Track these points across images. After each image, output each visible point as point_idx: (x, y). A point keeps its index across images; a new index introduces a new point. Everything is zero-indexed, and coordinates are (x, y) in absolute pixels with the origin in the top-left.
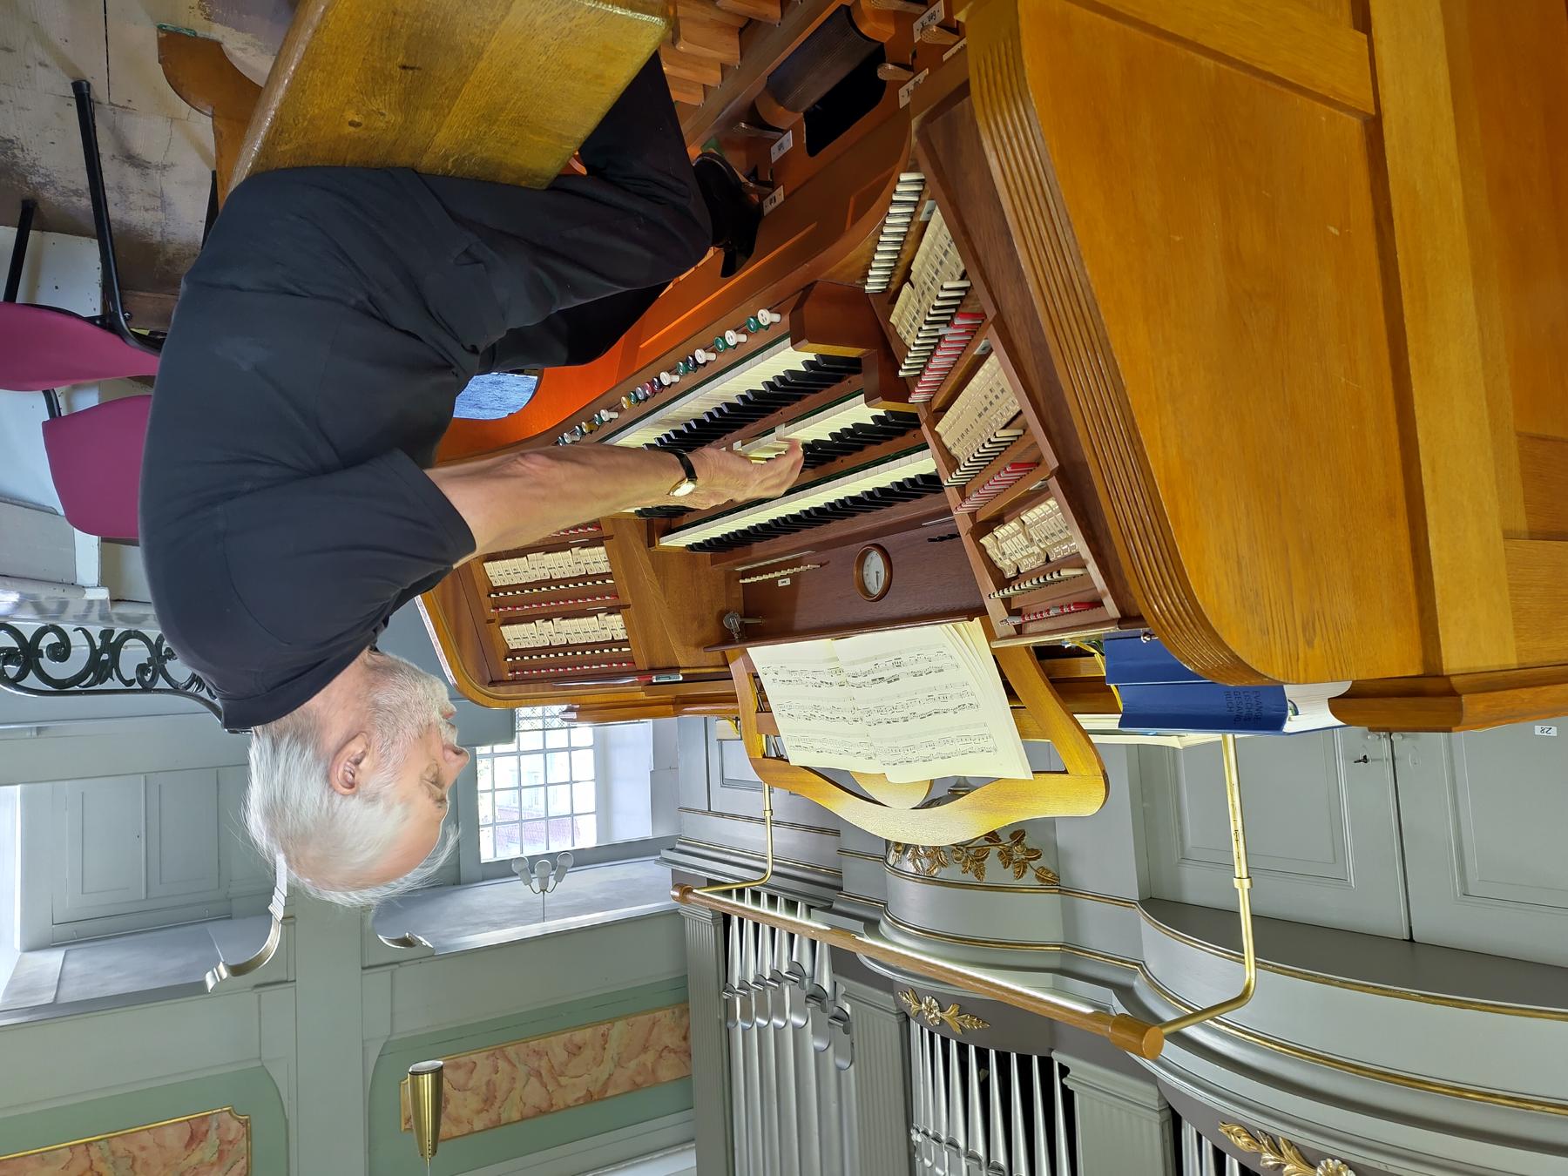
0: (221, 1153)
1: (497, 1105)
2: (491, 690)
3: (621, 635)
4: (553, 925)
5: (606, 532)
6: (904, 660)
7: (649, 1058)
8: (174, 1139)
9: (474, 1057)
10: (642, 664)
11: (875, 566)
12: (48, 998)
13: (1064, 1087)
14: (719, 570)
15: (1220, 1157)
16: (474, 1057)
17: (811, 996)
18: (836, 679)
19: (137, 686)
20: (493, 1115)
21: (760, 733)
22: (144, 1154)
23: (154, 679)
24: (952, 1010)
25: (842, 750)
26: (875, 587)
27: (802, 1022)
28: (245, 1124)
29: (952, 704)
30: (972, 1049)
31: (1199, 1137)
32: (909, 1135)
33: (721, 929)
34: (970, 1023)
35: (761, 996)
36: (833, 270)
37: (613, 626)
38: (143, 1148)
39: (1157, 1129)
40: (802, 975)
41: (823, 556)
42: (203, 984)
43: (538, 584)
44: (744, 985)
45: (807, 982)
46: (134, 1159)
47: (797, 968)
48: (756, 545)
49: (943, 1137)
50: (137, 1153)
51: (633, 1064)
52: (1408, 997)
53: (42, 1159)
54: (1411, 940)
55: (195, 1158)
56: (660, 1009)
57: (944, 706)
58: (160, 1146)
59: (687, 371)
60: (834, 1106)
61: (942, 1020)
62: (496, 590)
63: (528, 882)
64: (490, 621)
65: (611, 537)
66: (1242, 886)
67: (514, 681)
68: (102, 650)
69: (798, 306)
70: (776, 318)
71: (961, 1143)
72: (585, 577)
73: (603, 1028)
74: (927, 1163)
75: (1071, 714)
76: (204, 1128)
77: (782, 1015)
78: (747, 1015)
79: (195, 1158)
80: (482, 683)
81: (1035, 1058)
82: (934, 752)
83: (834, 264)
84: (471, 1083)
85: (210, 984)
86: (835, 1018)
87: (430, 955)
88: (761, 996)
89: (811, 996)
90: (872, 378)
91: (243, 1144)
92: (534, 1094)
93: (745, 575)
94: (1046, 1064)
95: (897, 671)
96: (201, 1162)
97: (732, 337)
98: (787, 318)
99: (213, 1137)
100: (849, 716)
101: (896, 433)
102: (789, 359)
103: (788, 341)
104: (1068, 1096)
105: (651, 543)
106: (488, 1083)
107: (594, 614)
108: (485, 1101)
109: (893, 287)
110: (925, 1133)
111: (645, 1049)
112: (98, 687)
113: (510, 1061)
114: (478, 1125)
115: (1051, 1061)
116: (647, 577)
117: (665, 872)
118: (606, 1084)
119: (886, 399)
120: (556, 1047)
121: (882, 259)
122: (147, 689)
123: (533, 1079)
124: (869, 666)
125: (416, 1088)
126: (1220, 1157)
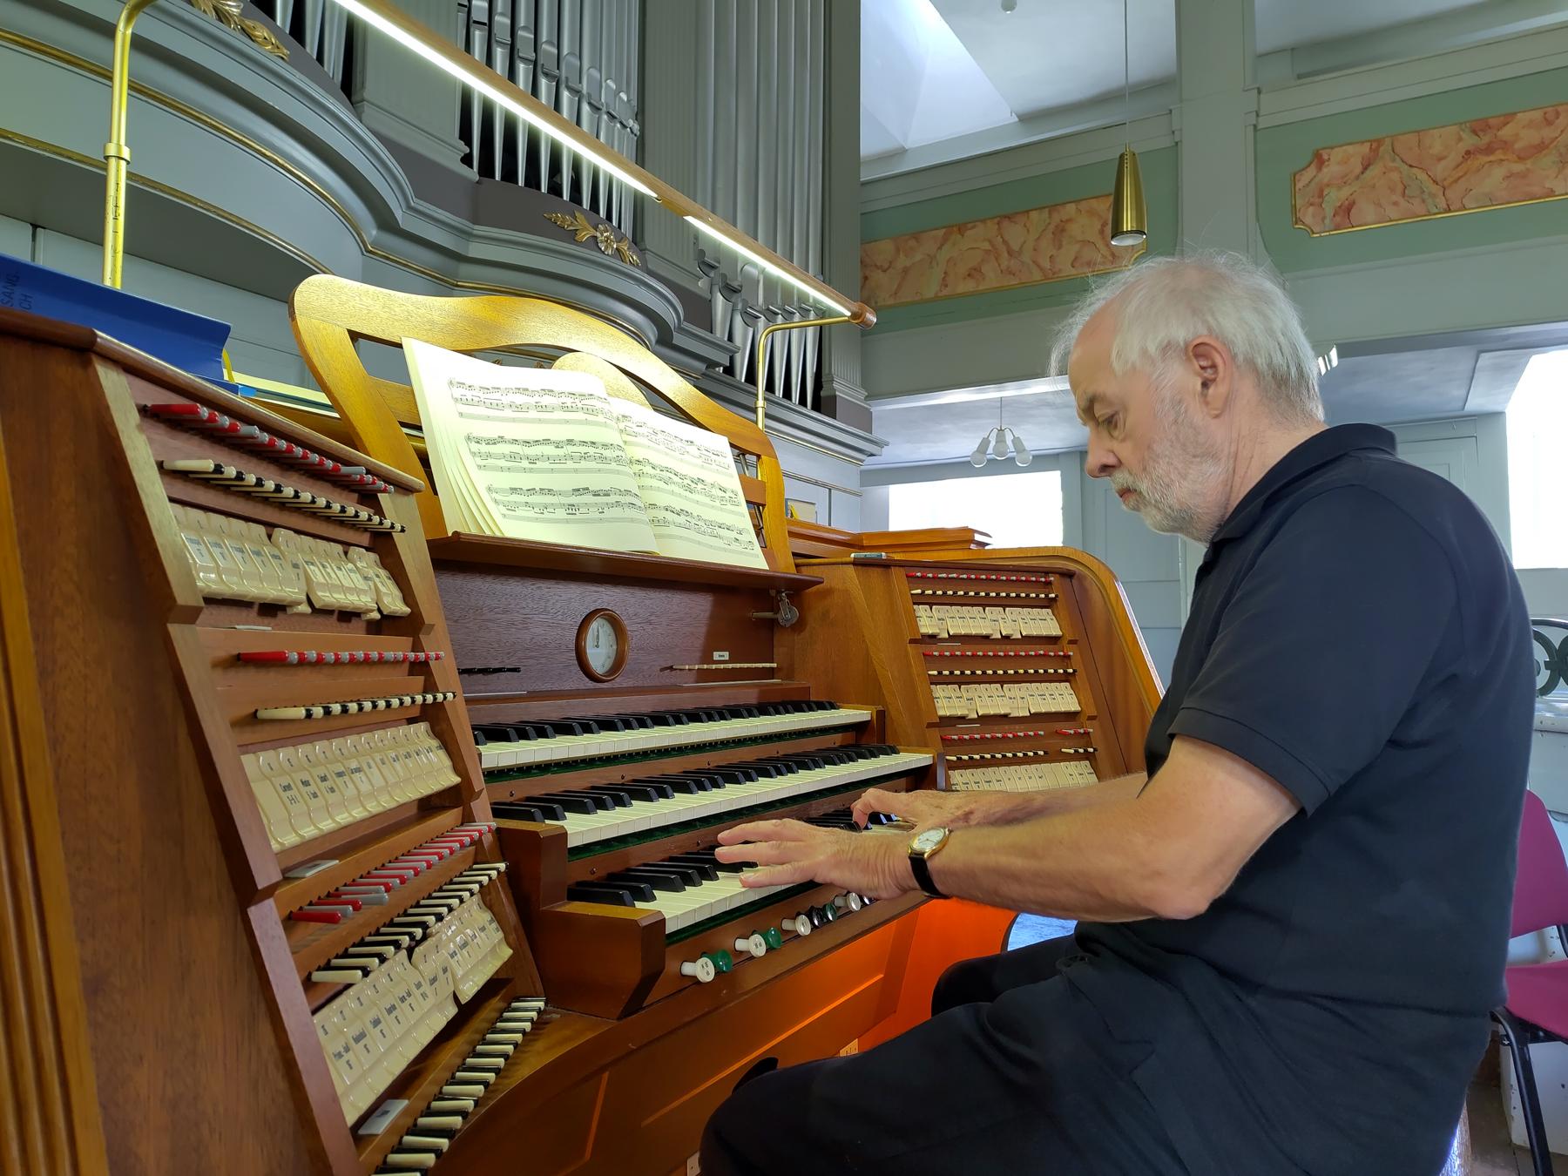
0: (1321, 195)
1: (1052, 227)
2: (1072, 567)
3: (922, 611)
4: (991, 393)
5: (935, 734)
6: (561, 513)
7: (902, 261)
8: (1366, 211)
9: (1073, 271)
10: (898, 575)
11: (600, 654)
12: (1485, 358)
13: (469, 143)
14: (794, 684)
15: (297, 29)
16: (1073, 271)
17: (736, 291)
18: (661, 514)
20: (1056, 218)
21: (762, 484)
22: (1394, 198)
24: (584, 236)
25: (660, 436)
26: (599, 628)
30: (566, 196)
31: (320, 58)
32: (642, 130)
33: (825, 371)
34: (567, 221)
36: (590, 1035)
37: (929, 621)
38: (1395, 204)
39: (368, 84)
40: (745, 313)
41: (668, 679)
42: (1340, 356)
43: (1017, 679)
46: (1404, 194)
48: (753, 701)
49: (605, 117)
50: (1401, 200)
51: (918, 257)
52: (28, 140)
53: (1492, 200)
54: (35, 226)
55: (1345, 192)
56: (891, 306)
58: (1380, 205)
59: (824, 909)
60: (720, 185)
61: (596, 228)
62: (1066, 678)
63: (1016, 441)
64: (1072, 642)
65: (930, 725)
66: (119, 145)
67: (1047, 573)
69: (649, 980)
70: (688, 968)
71: (586, 108)
72: (961, 681)
73: (945, 292)
74: (624, 96)
75: (344, 417)
76: (1338, 219)
80: (1082, 578)
81: (498, 176)
82: (537, 398)
83: (575, 1033)
84: (1077, 247)
85: (1334, 353)
86: (713, 267)
89: (736, 291)
90: (551, 872)
92: (1015, 234)
93: (770, 673)
94: (486, 169)
96: (1340, 188)
97: (755, 945)
98: (670, 966)
99: (1329, 212)
100: (648, 469)
101: (536, 798)
102: (677, 907)
103: (670, 928)
104: (465, 135)
105: (881, 715)
106: (1060, 247)
107: (952, 638)
108: (1063, 230)
109: (496, 1003)
110: (624, 126)
111: (906, 271)
114: (1071, 208)
115: (481, 173)
116: (888, 673)
117: (877, 434)
118: (945, 240)
119: (536, 834)
120: (992, 278)
121: (506, 1042)
123: (1016, 248)
124: (609, 513)
125: (1139, 217)
126: (297, 29)
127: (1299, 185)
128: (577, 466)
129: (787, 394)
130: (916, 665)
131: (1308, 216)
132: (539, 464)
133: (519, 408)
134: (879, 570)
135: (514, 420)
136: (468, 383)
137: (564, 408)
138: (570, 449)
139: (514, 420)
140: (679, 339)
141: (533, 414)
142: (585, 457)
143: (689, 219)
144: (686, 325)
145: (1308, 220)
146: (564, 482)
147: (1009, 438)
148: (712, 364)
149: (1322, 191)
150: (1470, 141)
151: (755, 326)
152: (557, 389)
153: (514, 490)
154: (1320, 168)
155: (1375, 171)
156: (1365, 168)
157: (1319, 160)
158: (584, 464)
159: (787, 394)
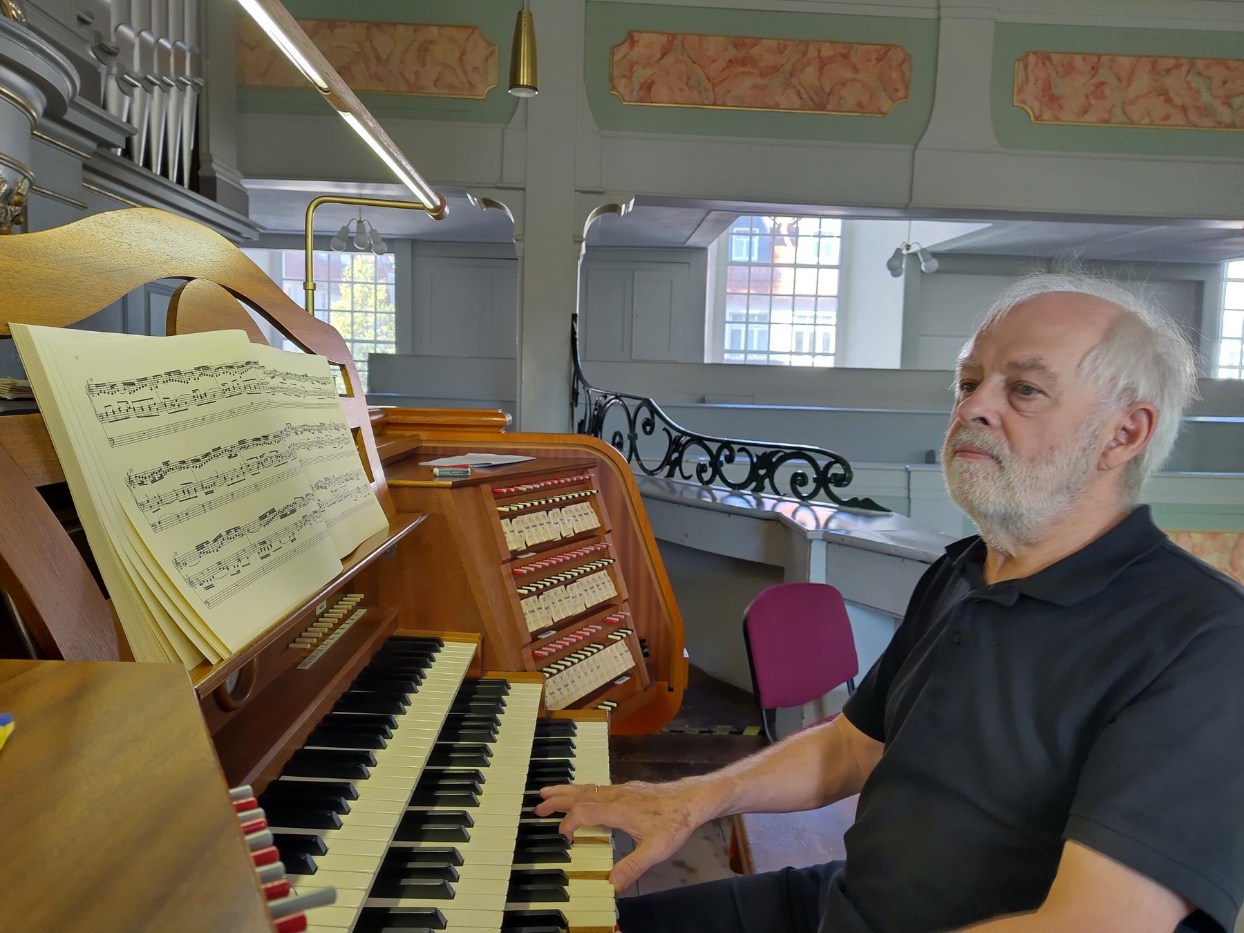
0: (631, 71)
6: (255, 558)
10: (486, 488)
19: (736, 447)
23: (720, 451)
27: (123, 28)
28: (614, 88)
29: (174, 481)
33: (202, 150)
35: (164, 70)
38: (681, 90)
40: (120, 80)
44: (182, 86)
45: (115, 70)
47: (126, 88)
55: (648, 72)
57: (187, 475)
63: (373, 232)
68: (763, 477)
76: (642, 93)
77: (144, 43)
78: (180, 55)
79: (648, 72)
82: (193, 384)
87: (472, 188)
88: (164, 70)
91: (616, 73)
95: (264, 533)
99: (636, 86)
106: (424, 65)
107: (530, 549)
108: (426, 50)
112: (769, 450)
113: (404, 78)
114: (434, 31)
117: (253, 217)
122: (726, 445)
123: (385, 57)
127: (617, 58)
128: (257, 478)
129: (165, 172)
130: (510, 584)
131: (622, 85)
132: (221, 491)
133: (174, 406)
134: (471, 490)
135: (174, 428)
136: (110, 380)
137: (227, 392)
138: (246, 454)
139: (174, 428)
140: (71, 115)
141: (194, 411)
142: (262, 462)
143: (349, 118)
144: (79, 100)
145: (621, 89)
146: (246, 510)
147: (368, 229)
148: (106, 145)
149: (632, 67)
150: (732, 53)
151: (131, 95)
152: (213, 363)
153: (200, 547)
154: (631, 47)
155: (669, 59)
156: (663, 55)
157: (631, 40)
158: (265, 473)
159: (165, 172)
